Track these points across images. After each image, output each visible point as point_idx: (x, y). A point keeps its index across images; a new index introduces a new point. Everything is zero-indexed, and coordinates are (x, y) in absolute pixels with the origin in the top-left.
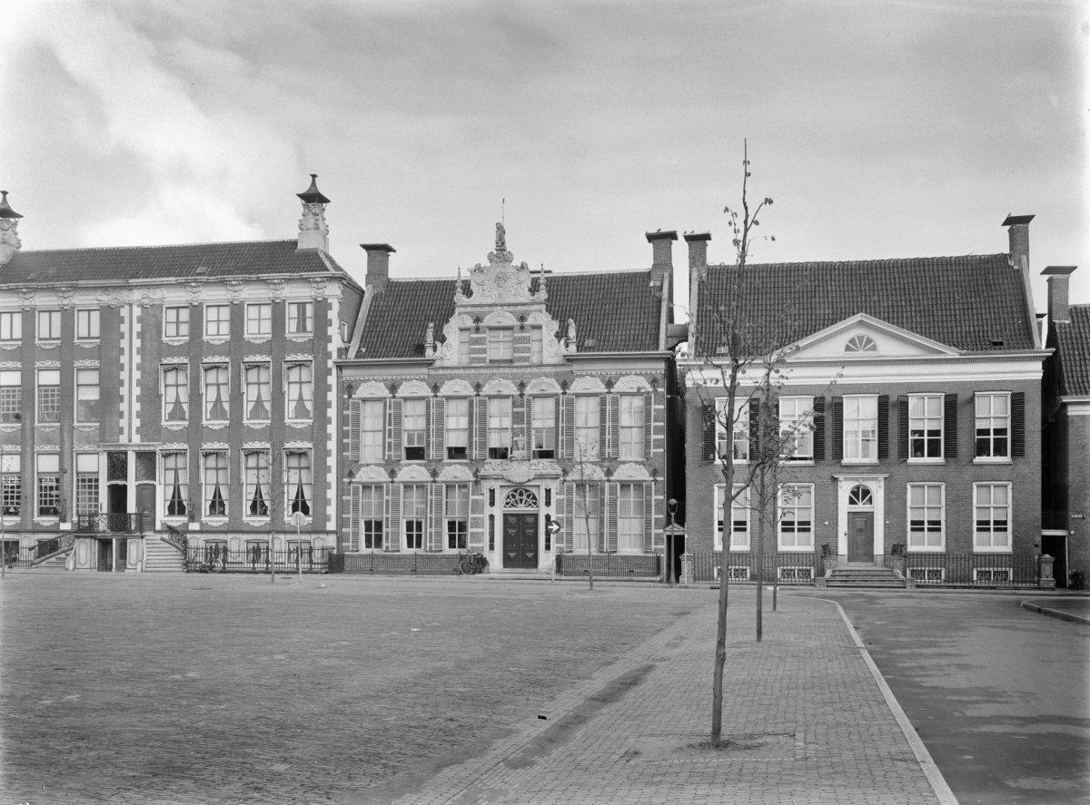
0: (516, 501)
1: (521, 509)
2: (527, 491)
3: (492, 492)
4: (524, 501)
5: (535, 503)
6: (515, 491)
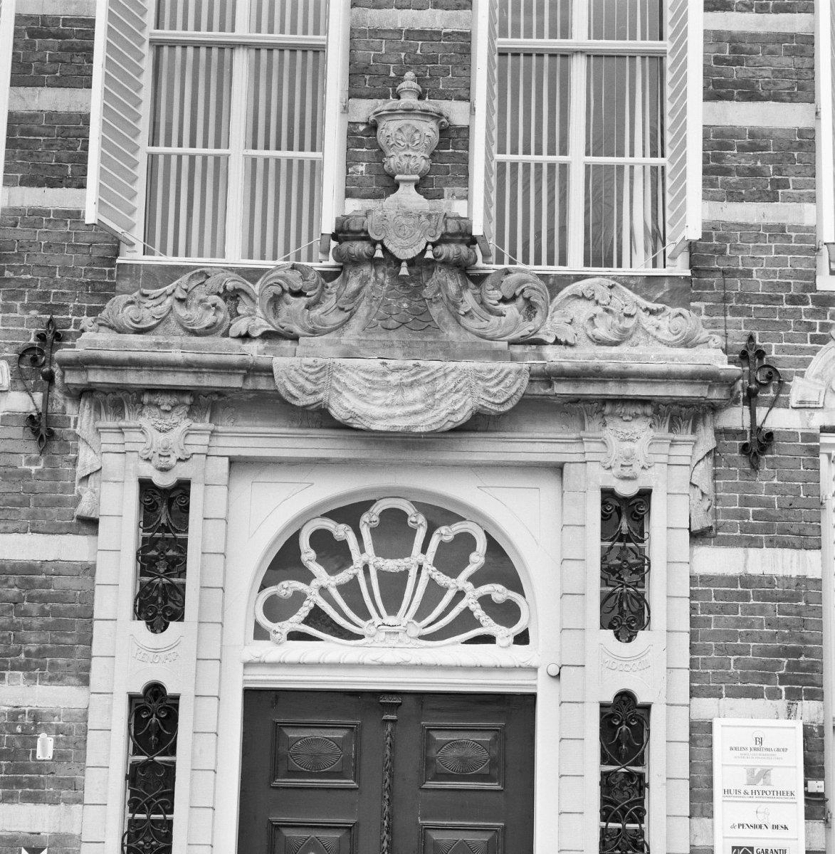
0: (350, 591)
1: (392, 654)
2: (439, 515)
3: (165, 507)
4: (414, 595)
5: (507, 614)
6: (349, 513)
